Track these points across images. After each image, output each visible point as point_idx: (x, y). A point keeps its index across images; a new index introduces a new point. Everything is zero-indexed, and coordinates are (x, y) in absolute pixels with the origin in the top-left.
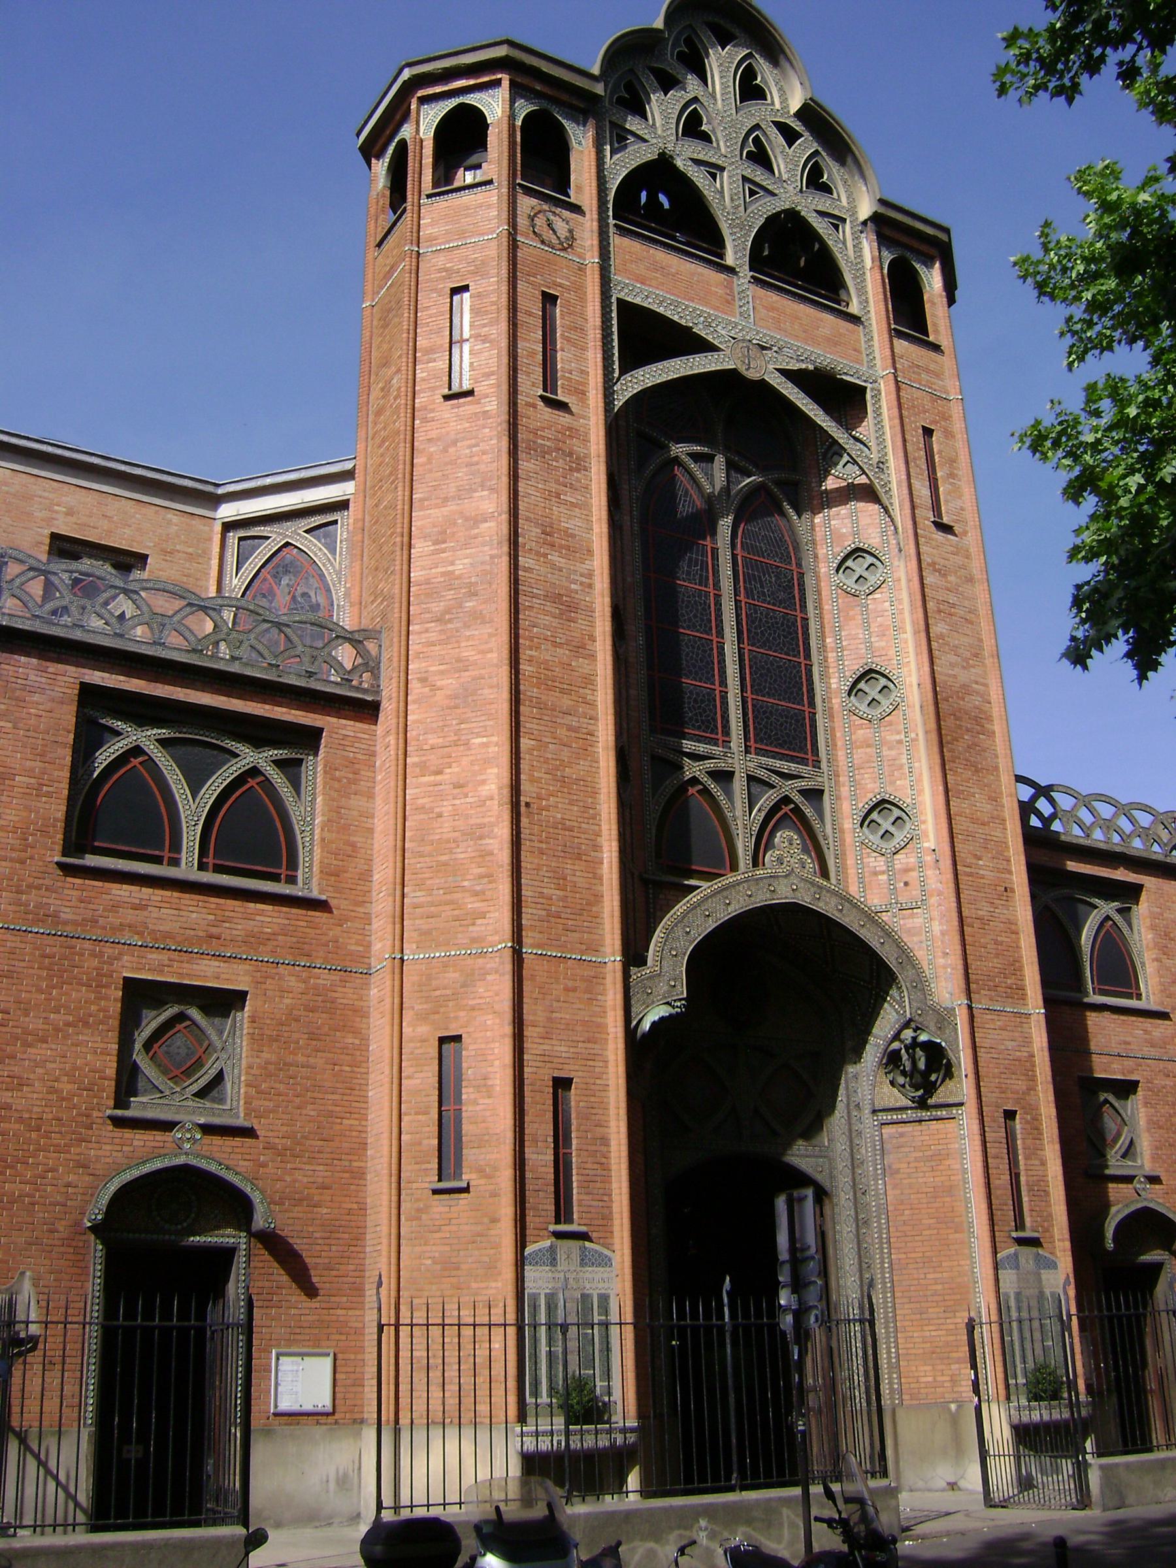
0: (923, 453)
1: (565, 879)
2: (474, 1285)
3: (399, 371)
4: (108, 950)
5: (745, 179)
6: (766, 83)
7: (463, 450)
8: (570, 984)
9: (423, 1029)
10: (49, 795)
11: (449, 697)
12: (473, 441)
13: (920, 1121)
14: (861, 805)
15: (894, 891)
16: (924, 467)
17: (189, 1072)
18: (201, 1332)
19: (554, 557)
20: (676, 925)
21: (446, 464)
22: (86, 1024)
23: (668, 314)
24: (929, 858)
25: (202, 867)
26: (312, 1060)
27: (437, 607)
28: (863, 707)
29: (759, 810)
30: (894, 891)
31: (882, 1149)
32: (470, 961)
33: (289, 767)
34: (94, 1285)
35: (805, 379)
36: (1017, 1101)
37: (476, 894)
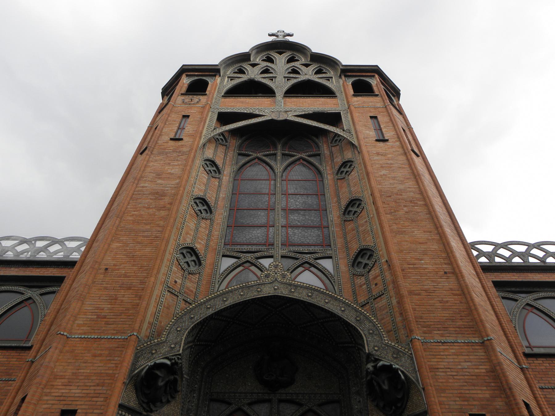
1: (116, 299)
5: (285, 77)
14: (351, 257)
19: (159, 181)
20: (185, 315)
30: (370, 291)
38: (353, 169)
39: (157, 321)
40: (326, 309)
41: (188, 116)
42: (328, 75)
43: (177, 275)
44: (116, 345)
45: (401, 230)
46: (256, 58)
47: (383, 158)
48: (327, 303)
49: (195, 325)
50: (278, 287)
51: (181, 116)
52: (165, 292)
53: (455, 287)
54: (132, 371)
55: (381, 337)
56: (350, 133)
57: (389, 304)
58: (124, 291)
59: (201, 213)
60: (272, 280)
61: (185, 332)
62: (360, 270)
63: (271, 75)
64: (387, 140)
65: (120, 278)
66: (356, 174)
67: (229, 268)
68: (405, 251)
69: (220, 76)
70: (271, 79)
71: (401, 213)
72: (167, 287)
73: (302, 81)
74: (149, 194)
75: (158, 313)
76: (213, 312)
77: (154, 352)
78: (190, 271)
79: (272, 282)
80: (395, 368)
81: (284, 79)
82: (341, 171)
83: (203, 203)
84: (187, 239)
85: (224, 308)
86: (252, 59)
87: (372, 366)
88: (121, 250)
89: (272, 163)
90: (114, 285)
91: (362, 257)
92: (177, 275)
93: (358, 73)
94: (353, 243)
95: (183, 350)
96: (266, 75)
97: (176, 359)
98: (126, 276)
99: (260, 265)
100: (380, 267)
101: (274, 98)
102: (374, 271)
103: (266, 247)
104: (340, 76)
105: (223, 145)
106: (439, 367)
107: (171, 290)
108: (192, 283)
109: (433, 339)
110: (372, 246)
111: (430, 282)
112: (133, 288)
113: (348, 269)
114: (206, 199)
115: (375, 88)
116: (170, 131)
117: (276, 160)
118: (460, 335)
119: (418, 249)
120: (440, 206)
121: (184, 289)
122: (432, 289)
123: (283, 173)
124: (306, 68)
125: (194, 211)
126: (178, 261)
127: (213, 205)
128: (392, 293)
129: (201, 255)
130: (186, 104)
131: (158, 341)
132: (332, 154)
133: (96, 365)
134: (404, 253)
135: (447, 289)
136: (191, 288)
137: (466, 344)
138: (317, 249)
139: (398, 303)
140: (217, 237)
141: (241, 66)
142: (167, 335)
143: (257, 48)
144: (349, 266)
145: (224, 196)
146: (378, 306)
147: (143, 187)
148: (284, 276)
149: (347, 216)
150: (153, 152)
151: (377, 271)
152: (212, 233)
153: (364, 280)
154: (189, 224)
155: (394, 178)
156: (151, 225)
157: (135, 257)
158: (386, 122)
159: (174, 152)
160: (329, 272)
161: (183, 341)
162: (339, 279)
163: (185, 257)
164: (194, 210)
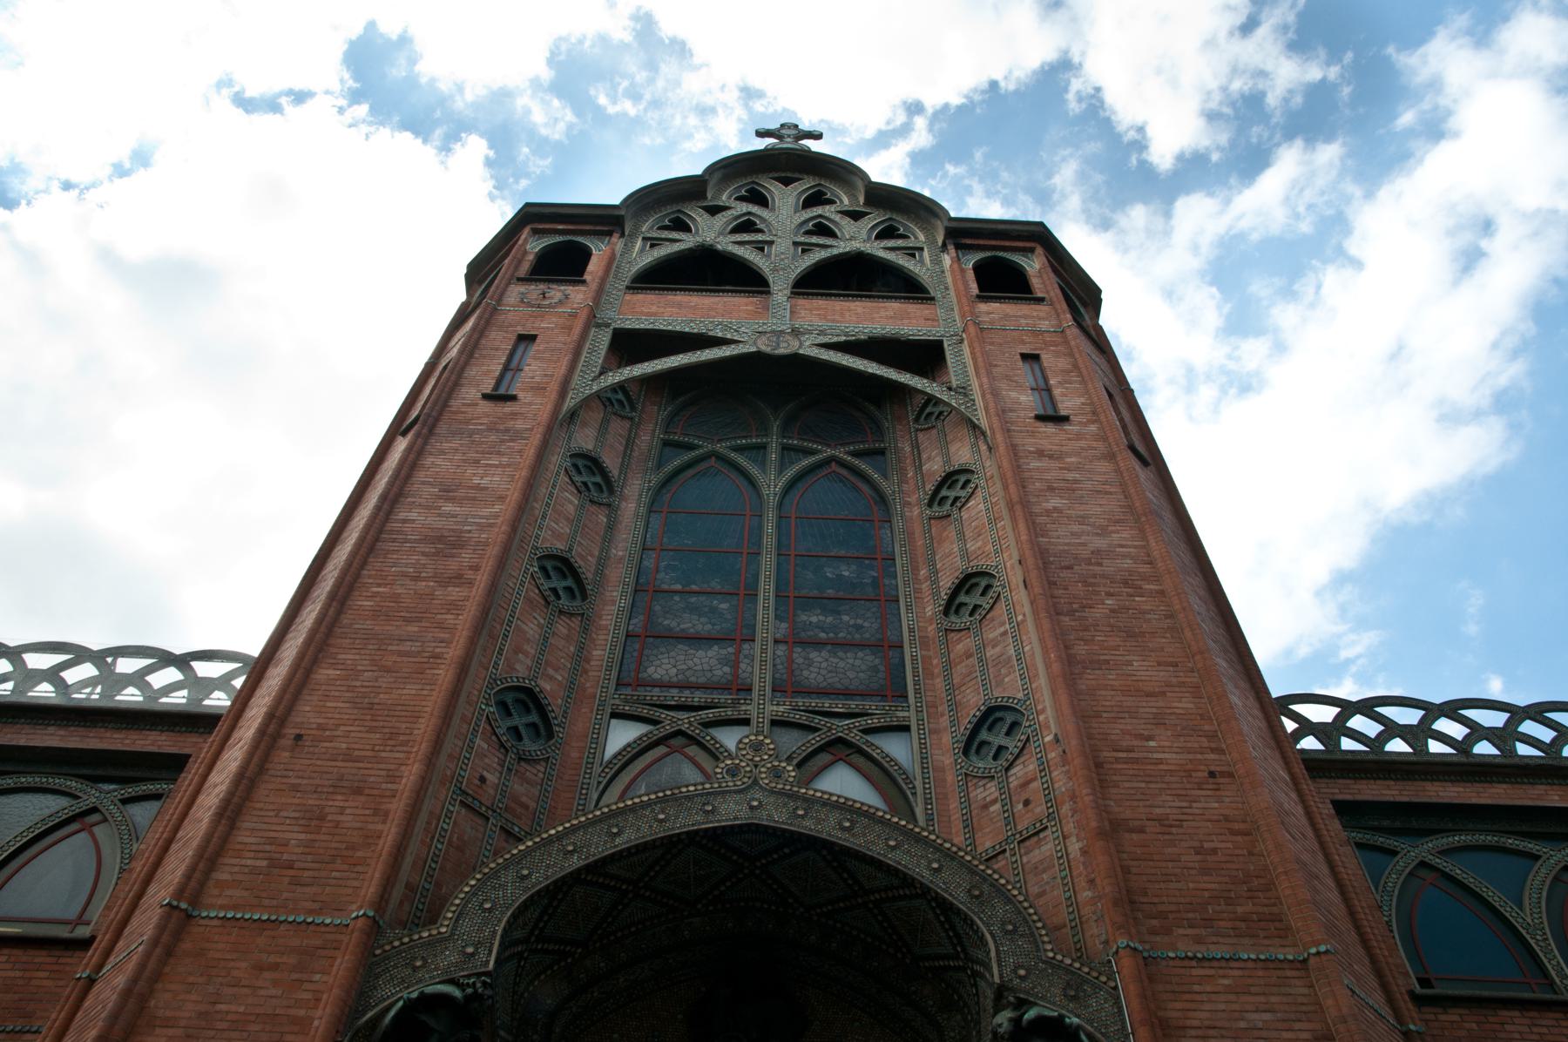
1: (322, 818)
5: (796, 244)
19: (448, 508)
20: (506, 867)
30: (1010, 819)
38: (973, 493)
39: (430, 883)
40: (889, 865)
41: (531, 338)
42: (911, 243)
43: (487, 760)
44: (318, 942)
45: (1096, 657)
46: (720, 191)
47: (1056, 464)
48: (894, 848)
49: (532, 896)
50: (760, 802)
51: (514, 337)
52: (454, 806)
53: (1236, 813)
55: (1035, 942)
56: (965, 395)
57: (1059, 854)
58: (343, 798)
59: (559, 598)
60: (744, 783)
61: (503, 913)
62: (981, 764)
63: (759, 237)
64: (1065, 419)
65: (333, 763)
66: (982, 506)
67: (629, 749)
68: (1105, 715)
69: (623, 235)
70: (760, 247)
71: (1098, 613)
72: (458, 792)
73: (841, 255)
74: (419, 541)
75: (432, 860)
76: (582, 863)
77: (419, 963)
78: (521, 752)
79: (744, 789)
80: (1071, 1024)
81: (792, 248)
82: (941, 496)
83: (565, 569)
84: (518, 667)
85: (613, 854)
86: (709, 195)
87: (1010, 1020)
88: (339, 688)
89: (754, 471)
90: (318, 782)
91: (990, 729)
92: (487, 760)
93: (990, 239)
94: (968, 691)
95: (496, 962)
96: (746, 237)
97: (479, 985)
98: (348, 757)
99: (712, 742)
100: (1039, 755)
101: (764, 296)
102: (1022, 766)
103: (731, 694)
104: (944, 245)
105: (623, 417)
106: (1188, 1023)
107: (470, 800)
108: (525, 785)
109: (1175, 950)
110: (1019, 700)
111: (1169, 798)
112: (367, 791)
113: (952, 759)
114: (572, 560)
115: (1036, 283)
116: (484, 375)
117: (763, 465)
118: (1246, 941)
119: (1141, 710)
120: (1200, 598)
121: (505, 800)
122: (1175, 817)
123: (783, 498)
124: (852, 222)
125: (537, 591)
126: (490, 725)
127: (590, 576)
128: (1070, 827)
129: (553, 711)
130: (529, 305)
131: (430, 935)
132: (919, 450)
133: (262, 992)
134: (1105, 720)
135: (1215, 818)
136: (524, 799)
137: (1260, 965)
138: (870, 705)
140: (600, 663)
141: (679, 211)
142: (457, 920)
143: (725, 167)
144: (956, 751)
145: (621, 553)
146: (1028, 862)
147: (405, 521)
148: (777, 774)
149: (953, 618)
150: (437, 430)
151: (1031, 767)
152: (585, 652)
153: (994, 789)
154: (524, 626)
155: (1082, 520)
156: (423, 624)
157: (376, 707)
158: (1062, 371)
159: (489, 430)
160: (900, 768)
161: (498, 937)
162: (927, 786)
163: (509, 714)
164: (539, 588)
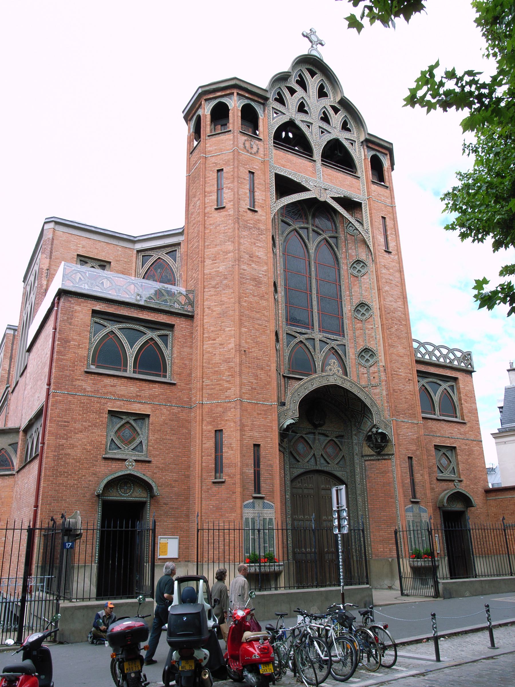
0: (382, 226)
1: (257, 376)
2: (227, 515)
3: (199, 199)
4: (103, 401)
6: (328, 90)
7: (222, 228)
8: (259, 412)
9: (210, 427)
10: (82, 348)
11: (217, 314)
12: (225, 225)
13: (379, 460)
15: (369, 380)
16: (382, 231)
17: (130, 442)
18: (133, 533)
19: (253, 265)
21: (216, 233)
22: (96, 426)
23: (293, 178)
24: (382, 369)
25: (134, 372)
26: (172, 438)
27: (213, 283)
28: (359, 316)
29: (324, 352)
30: (369, 380)
31: (365, 469)
32: (225, 404)
33: (164, 337)
34: (98, 516)
35: (340, 200)
36: (413, 454)
37: (227, 381)
54: (279, 425)
74: (250, 280)
139: (387, 395)
